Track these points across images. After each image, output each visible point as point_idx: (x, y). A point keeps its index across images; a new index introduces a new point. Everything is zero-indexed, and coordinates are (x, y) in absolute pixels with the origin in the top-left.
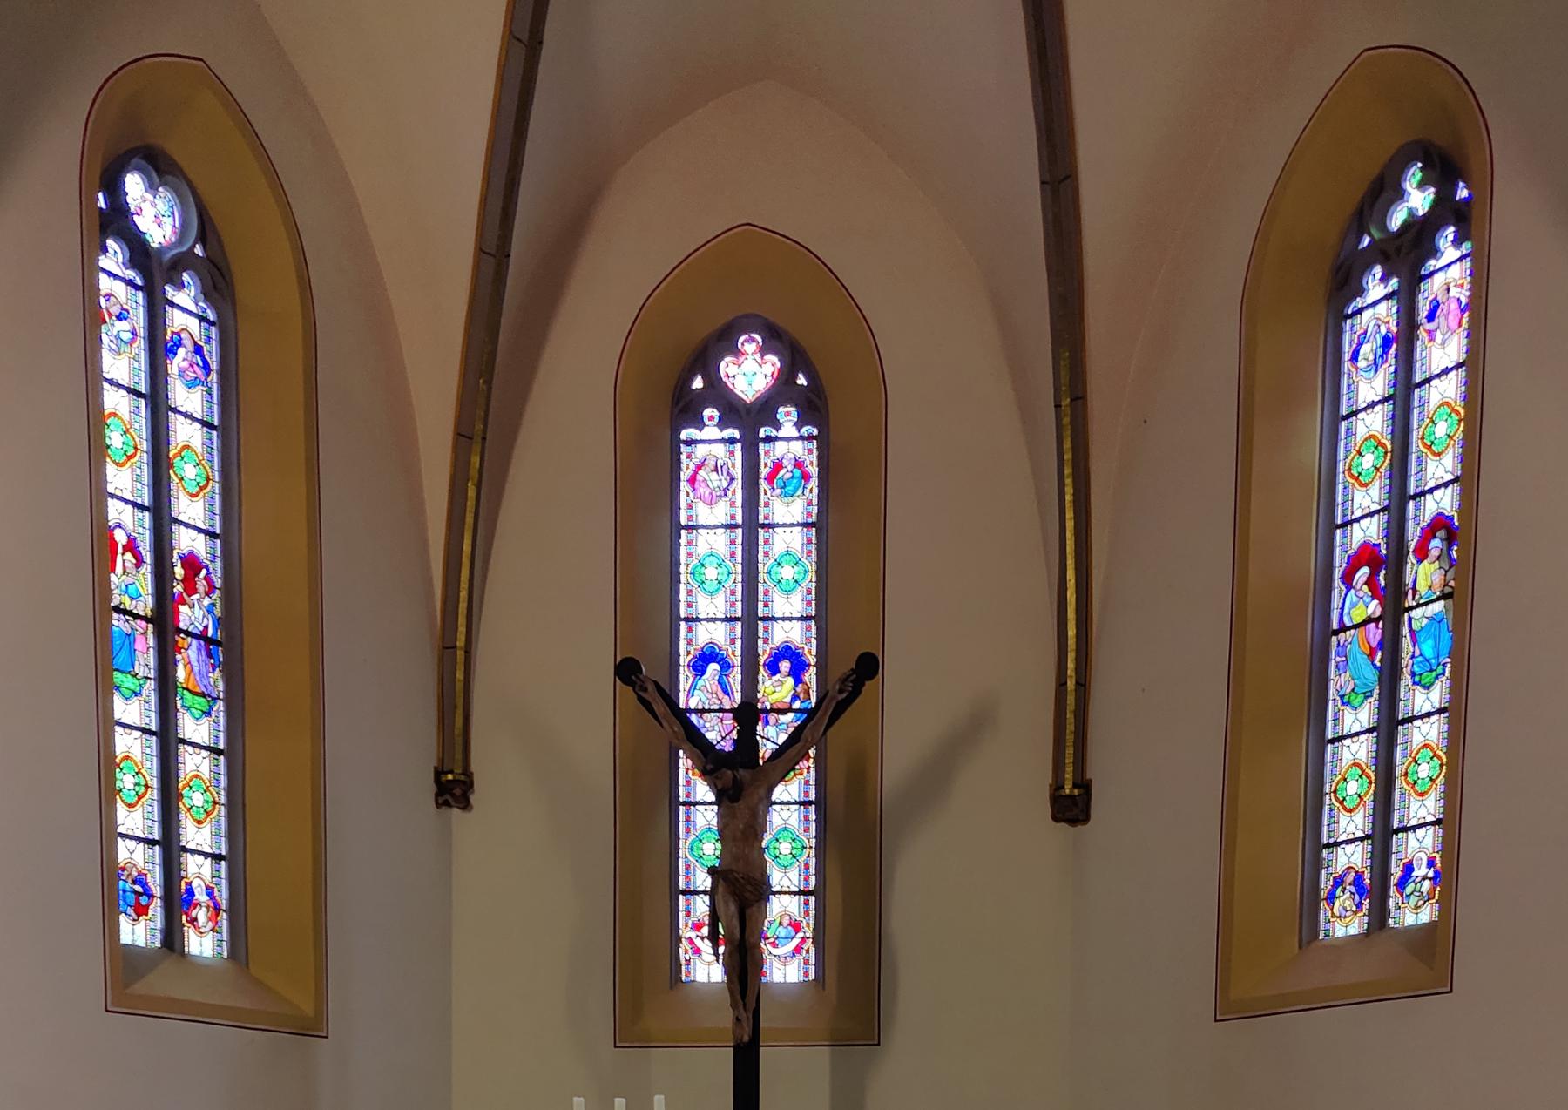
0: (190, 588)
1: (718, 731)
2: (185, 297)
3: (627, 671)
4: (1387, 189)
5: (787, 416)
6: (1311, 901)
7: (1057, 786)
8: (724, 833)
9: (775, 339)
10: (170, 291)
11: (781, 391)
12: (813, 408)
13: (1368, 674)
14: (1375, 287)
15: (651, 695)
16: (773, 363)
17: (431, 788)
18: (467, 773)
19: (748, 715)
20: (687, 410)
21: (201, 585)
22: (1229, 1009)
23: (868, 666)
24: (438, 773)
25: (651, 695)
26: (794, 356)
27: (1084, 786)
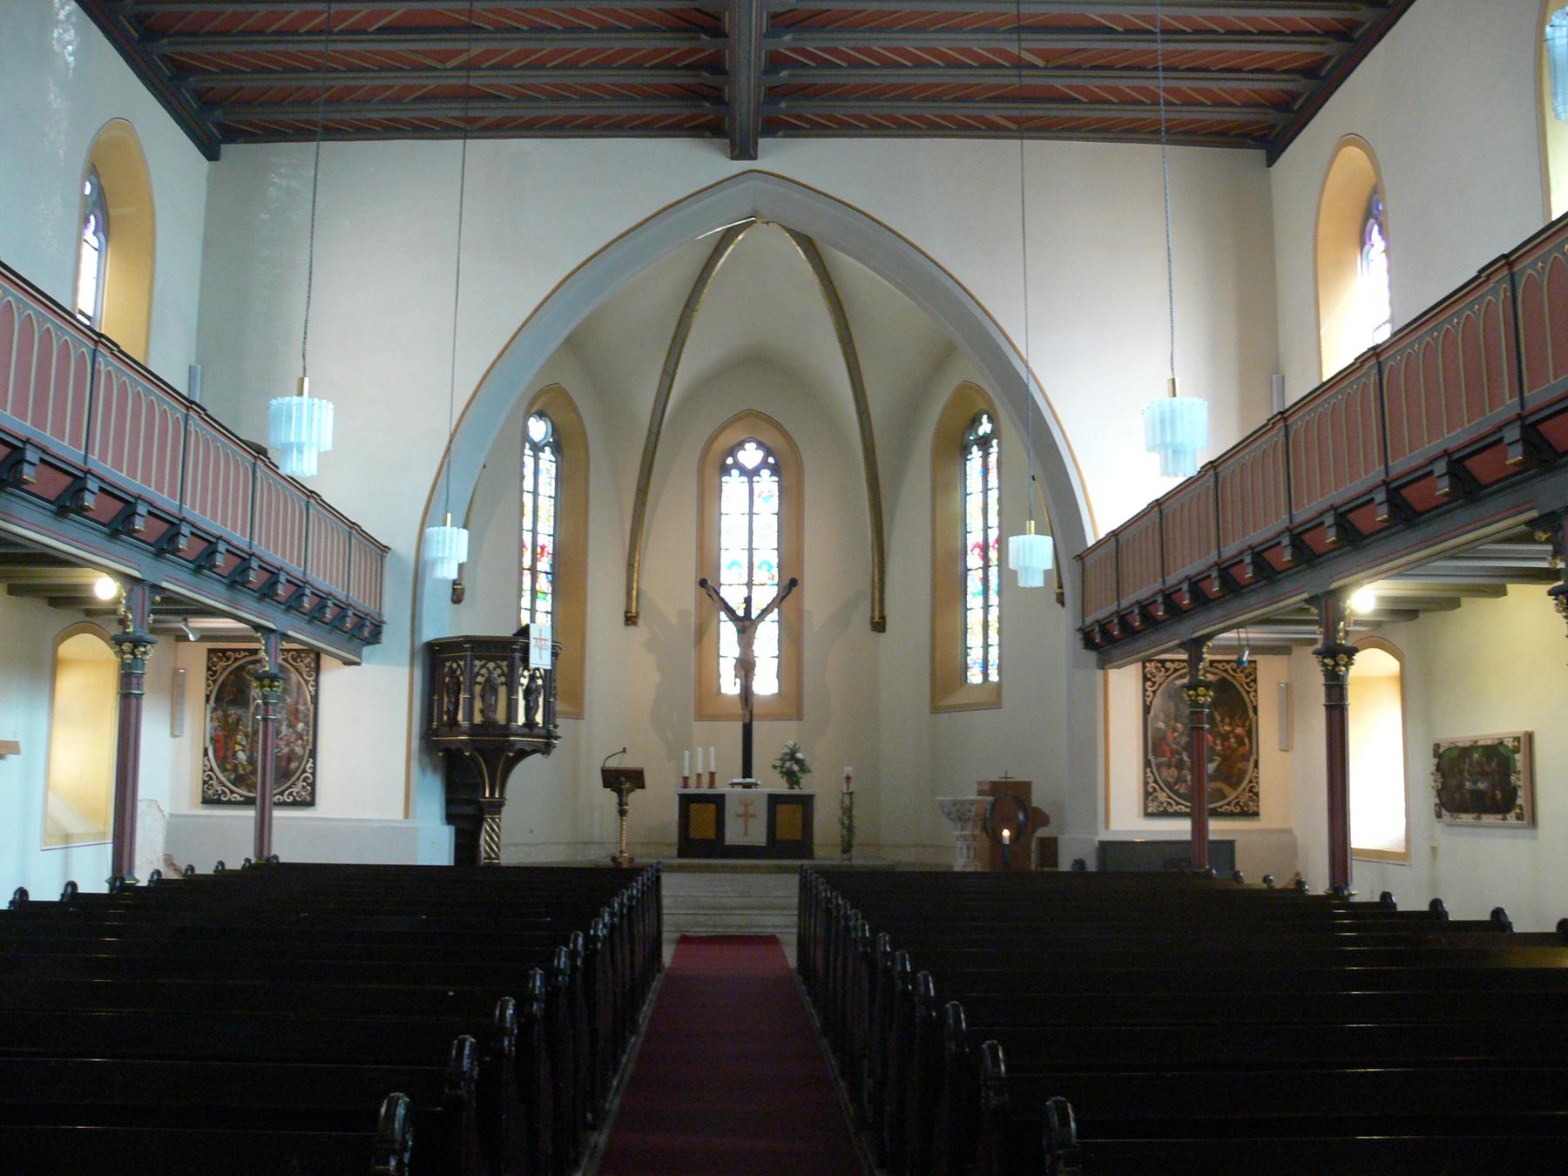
0: (542, 554)
1: (736, 603)
2: (547, 456)
3: (703, 583)
4: (975, 422)
5: (765, 473)
6: (966, 667)
7: (873, 618)
8: (740, 642)
9: (761, 445)
10: (541, 454)
11: (764, 464)
12: (775, 470)
13: (980, 587)
14: (976, 453)
15: (712, 593)
16: (760, 454)
17: (624, 619)
18: (637, 613)
19: (748, 601)
20: (725, 470)
21: (545, 554)
22: (935, 709)
23: (793, 583)
24: (626, 612)
25: (712, 593)
26: (769, 452)
27: (883, 617)
